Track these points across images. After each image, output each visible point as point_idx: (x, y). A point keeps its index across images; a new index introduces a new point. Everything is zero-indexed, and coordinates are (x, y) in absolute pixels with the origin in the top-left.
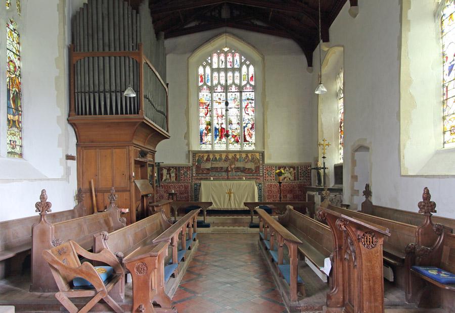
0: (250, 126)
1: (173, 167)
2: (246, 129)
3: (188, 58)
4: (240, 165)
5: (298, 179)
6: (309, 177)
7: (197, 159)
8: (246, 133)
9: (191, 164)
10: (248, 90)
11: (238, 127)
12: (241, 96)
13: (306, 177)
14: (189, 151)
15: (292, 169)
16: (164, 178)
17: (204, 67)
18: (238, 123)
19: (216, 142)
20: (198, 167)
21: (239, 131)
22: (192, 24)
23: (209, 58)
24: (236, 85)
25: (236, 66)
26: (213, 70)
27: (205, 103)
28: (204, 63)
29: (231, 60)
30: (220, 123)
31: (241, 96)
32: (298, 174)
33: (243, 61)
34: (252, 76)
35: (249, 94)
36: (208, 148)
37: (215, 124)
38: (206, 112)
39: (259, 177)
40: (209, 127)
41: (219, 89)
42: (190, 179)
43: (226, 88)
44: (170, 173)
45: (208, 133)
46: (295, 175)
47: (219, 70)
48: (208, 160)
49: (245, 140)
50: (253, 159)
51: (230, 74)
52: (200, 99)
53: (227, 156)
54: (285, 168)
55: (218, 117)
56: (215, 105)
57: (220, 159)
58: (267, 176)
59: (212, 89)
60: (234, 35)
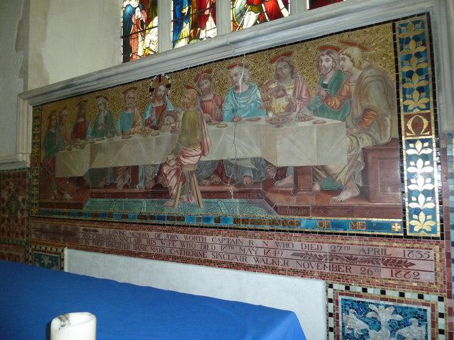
39: (397, 250)
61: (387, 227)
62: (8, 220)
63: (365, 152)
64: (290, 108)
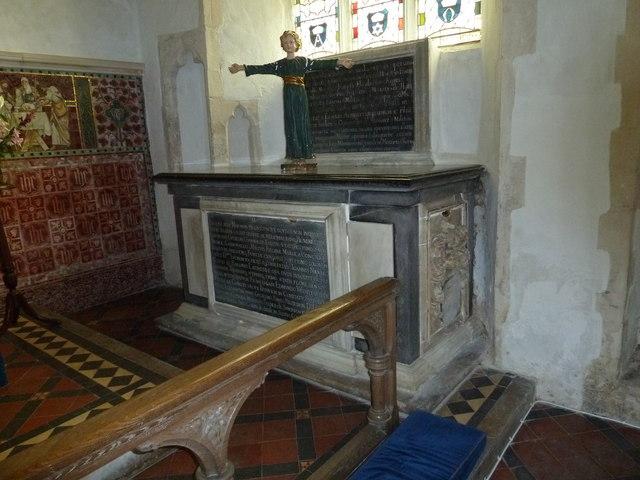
6: (137, 128)
13: (127, 128)
46: (73, 122)
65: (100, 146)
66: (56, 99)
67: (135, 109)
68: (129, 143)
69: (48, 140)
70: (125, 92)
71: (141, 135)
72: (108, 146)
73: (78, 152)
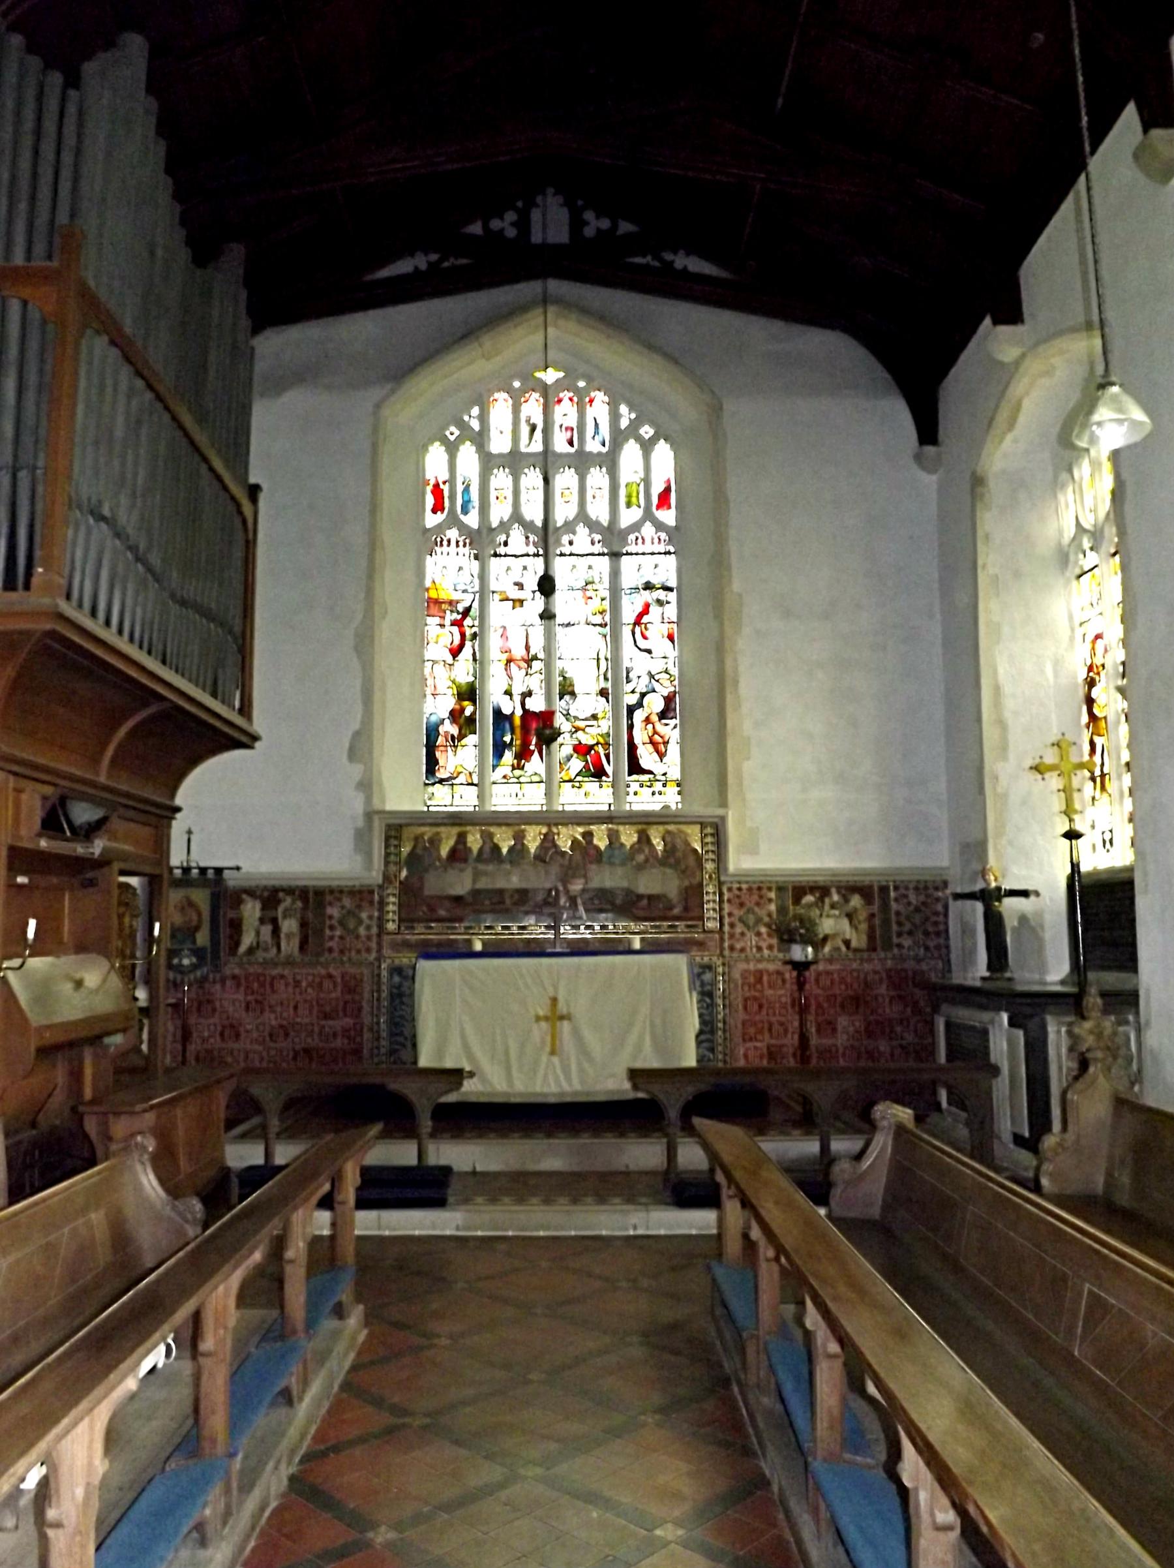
0: (655, 704)
1: (290, 891)
2: (639, 716)
3: (378, 406)
4: (609, 878)
5: (888, 945)
7: (405, 850)
8: (640, 736)
9: (375, 876)
10: (648, 548)
11: (602, 706)
12: (615, 574)
13: (926, 934)
14: (369, 815)
15: (856, 901)
16: (247, 940)
17: (452, 449)
18: (603, 693)
19: (497, 775)
20: (410, 893)
21: (605, 725)
22: (404, 267)
23: (475, 411)
24: (593, 526)
25: (593, 446)
26: (488, 462)
27: (451, 603)
28: (453, 432)
29: (572, 421)
30: (517, 690)
31: (615, 574)
32: (886, 922)
33: (624, 423)
34: (667, 491)
35: (653, 564)
36: (465, 800)
37: (495, 695)
38: (457, 641)
40: (469, 711)
41: (517, 540)
42: (374, 945)
43: (546, 537)
44: (274, 922)
45: (462, 736)
47: (515, 461)
48: (459, 854)
49: (635, 767)
50: (670, 850)
51: (565, 479)
52: (428, 583)
53: (548, 841)
54: (822, 891)
55: (509, 661)
56: (498, 612)
57: (519, 850)
58: (739, 929)
59: (483, 543)
60: (584, 311)
61: (455, 928)
62: (341, 938)
63: (686, 889)
64: (647, 861)
65: (896, 951)
66: (858, 906)
67: (937, 914)
68: (927, 948)
69: (847, 943)
70: (927, 896)
71: (942, 941)
72: (905, 951)
73: (874, 955)
